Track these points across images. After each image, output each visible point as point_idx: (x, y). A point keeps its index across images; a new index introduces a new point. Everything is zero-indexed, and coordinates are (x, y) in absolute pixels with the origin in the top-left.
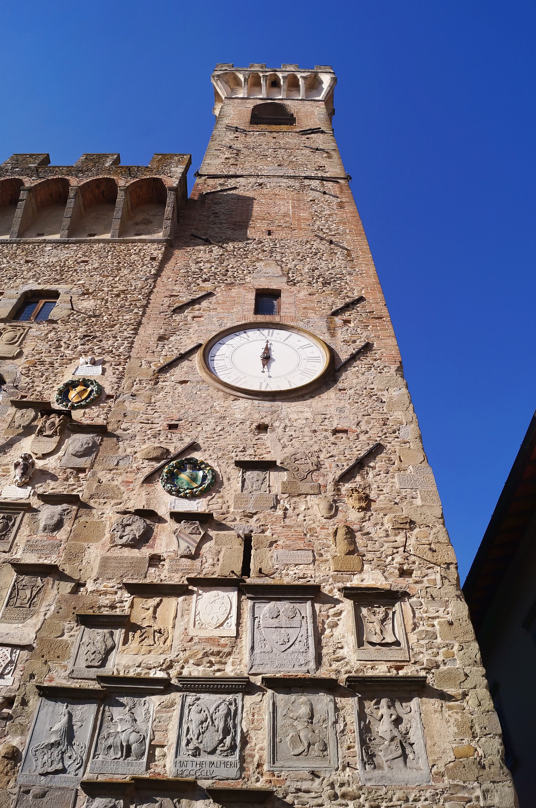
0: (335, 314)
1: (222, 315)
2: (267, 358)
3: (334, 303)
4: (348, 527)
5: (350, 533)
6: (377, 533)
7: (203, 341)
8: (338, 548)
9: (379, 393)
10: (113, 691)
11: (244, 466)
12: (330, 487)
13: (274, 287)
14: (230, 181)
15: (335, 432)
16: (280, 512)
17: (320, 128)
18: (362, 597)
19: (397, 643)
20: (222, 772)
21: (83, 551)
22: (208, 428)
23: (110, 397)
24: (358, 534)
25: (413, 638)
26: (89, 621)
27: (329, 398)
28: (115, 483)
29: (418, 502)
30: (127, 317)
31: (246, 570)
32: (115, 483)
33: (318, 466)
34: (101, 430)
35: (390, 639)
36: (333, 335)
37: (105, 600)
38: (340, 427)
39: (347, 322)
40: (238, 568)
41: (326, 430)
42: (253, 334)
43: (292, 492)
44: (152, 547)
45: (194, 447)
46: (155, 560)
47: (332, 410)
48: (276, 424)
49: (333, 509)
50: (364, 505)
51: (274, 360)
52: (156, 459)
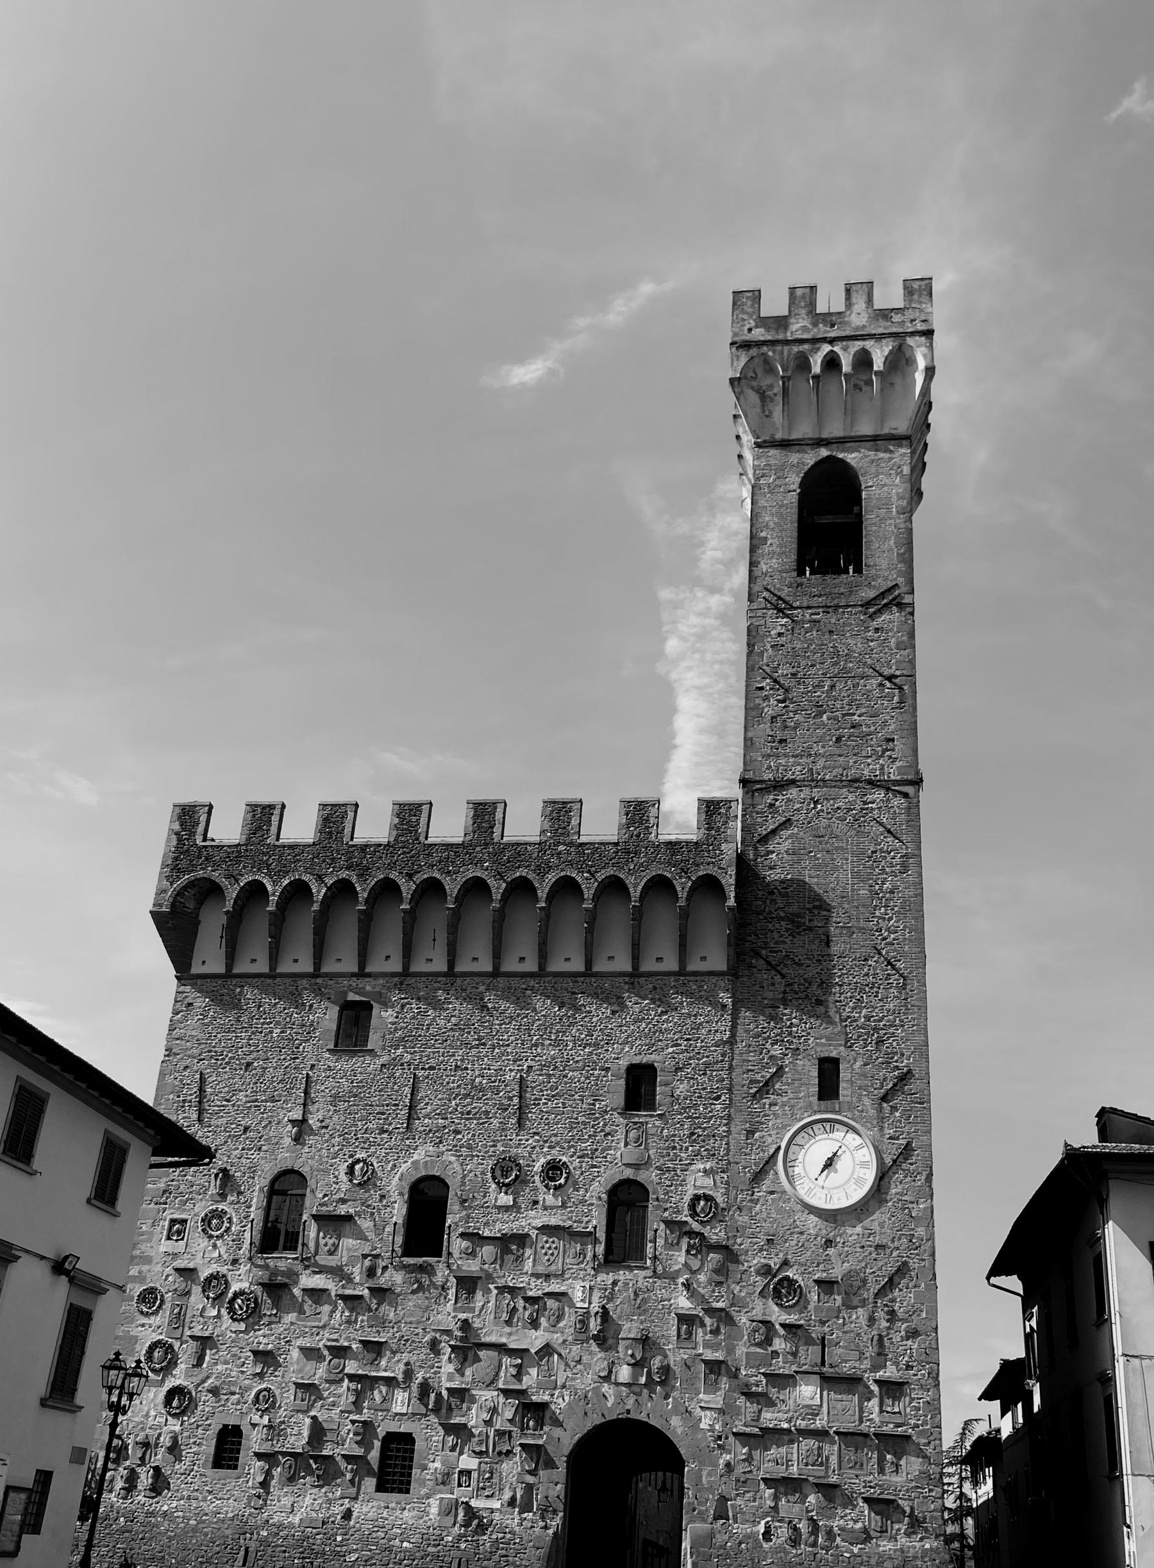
0: (884, 1098)
3: (885, 1080)
4: (880, 1335)
5: (881, 1337)
6: (896, 1338)
8: (870, 1351)
9: (911, 1206)
13: (834, 1054)
15: (878, 1247)
16: (841, 1321)
19: (900, 1413)
21: (734, 1347)
22: (793, 1243)
25: (908, 1410)
29: (924, 1315)
31: (823, 1363)
32: (743, 1294)
33: (864, 1281)
35: (896, 1410)
37: (753, 1380)
39: (894, 1109)
40: (819, 1361)
41: (870, 1246)
45: (785, 1263)
46: (775, 1354)
47: (876, 1227)
49: (872, 1320)
51: (836, 1171)
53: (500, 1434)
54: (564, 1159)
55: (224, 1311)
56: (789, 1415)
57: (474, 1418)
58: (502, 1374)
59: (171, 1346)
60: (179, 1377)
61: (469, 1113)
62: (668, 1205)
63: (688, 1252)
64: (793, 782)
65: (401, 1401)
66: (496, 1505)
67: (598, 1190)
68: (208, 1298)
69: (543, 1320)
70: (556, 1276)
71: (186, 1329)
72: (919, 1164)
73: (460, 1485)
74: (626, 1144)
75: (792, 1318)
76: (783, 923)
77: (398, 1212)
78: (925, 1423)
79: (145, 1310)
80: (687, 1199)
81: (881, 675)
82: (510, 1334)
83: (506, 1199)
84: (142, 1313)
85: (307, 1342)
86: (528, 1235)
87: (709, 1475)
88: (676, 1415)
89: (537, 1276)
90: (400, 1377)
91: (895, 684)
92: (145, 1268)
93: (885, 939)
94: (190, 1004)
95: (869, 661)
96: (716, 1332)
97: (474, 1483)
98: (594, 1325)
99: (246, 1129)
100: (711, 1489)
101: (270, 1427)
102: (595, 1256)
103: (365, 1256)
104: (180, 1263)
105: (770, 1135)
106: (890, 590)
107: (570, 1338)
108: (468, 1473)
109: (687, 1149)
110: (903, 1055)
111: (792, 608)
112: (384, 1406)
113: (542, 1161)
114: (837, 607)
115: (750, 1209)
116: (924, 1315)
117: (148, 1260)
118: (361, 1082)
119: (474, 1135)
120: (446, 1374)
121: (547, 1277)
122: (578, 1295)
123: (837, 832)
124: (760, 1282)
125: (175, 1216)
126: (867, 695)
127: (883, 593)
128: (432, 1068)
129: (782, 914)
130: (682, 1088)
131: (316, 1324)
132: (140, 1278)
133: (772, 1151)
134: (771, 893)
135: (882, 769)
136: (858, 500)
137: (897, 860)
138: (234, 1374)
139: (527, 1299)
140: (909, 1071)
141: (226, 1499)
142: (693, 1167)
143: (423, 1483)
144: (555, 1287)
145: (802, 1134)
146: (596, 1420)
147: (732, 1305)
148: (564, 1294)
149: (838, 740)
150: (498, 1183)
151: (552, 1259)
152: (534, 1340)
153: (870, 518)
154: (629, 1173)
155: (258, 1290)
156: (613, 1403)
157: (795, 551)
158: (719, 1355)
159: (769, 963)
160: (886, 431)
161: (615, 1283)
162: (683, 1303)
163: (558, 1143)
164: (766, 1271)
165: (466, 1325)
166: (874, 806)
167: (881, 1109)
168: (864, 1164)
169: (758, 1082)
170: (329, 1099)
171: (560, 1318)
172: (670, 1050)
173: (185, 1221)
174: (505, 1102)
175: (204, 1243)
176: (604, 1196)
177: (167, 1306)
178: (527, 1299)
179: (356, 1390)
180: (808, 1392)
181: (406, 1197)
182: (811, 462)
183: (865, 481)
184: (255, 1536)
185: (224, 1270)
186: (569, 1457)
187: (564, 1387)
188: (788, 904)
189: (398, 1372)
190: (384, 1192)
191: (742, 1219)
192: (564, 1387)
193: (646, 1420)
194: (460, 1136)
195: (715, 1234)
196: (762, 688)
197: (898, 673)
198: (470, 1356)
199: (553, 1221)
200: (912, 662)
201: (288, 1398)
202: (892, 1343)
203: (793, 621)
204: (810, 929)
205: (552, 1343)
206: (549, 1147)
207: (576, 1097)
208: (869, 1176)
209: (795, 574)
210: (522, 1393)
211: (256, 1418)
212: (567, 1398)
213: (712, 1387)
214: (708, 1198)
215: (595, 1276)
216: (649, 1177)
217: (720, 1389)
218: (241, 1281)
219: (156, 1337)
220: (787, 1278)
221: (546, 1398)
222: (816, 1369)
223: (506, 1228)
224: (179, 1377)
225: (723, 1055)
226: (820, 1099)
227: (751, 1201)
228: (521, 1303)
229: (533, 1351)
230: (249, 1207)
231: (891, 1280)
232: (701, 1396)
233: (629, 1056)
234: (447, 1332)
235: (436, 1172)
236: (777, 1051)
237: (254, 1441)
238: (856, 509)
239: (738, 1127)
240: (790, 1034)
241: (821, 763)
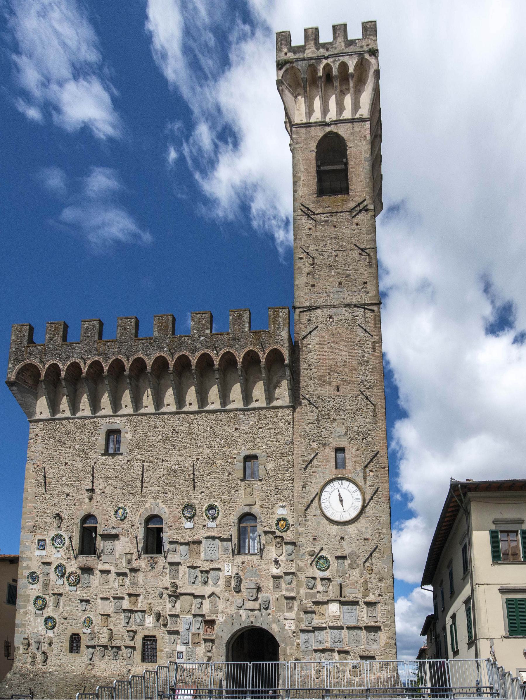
0: (366, 467)
1: (323, 470)
2: (341, 501)
7: (318, 491)
10: (315, 629)
11: (338, 558)
12: (362, 565)
13: (342, 445)
14: (314, 314)
15: (365, 539)
17: (365, 200)
18: (369, 604)
20: (339, 646)
23: (292, 525)
24: (369, 583)
26: (306, 612)
27: (362, 520)
28: (302, 565)
30: (288, 475)
31: (341, 596)
34: (294, 544)
36: (365, 483)
37: (308, 605)
38: (366, 537)
41: (361, 539)
42: (336, 484)
43: (351, 567)
44: (316, 589)
45: (322, 549)
47: (363, 529)
48: (346, 537)
50: (370, 572)
52: (312, 555)
53: (194, 634)
54: (216, 504)
55: (66, 582)
56: (326, 621)
57: (182, 627)
58: (193, 607)
59: (44, 598)
60: (49, 612)
61: (170, 483)
62: (266, 524)
63: (276, 545)
64: (319, 307)
65: (149, 621)
66: (195, 666)
67: (234, 518)
68: (58, 576)
69: (210, 581)
71: (50, 590)
72: (383, 497)
73: (178, 658)
74: (245, 495)
75: (326, 574)
76: (316, 380)
77: (141, 533)
78: (387, 620)
79: (32, 582)
80: (275, 521)
81: (359, 248)
82: (196, 589)
83: (190, 525)
84: (30, 583)
85: (105, 595)
87: (290, 649)
88: (274, 623)
90: (147, 610)
91: (366, 253)
92: (29, 563)
93: (365, 386)
94: (37, 435)
95: (354, 241)
96: (290, 583)
97: (184, 657)
98: (233, 584)
99: (68, 495)
100: (291, 656)
101: (91, 633)
103: (126, 554)
104: (45, 560)
105: (313, 488)
106: (362, 203)
107: (224, 590)
108: (182, 652)
109: (274, 496)
110: (375, 444)
111: (314, 214)
112: (141, 624)
113: (206, 505)
114: (337, 212)
115: (305, 524)
116: (386, 570)
117: (30, 559)
118: (118, 469)
119: (173, 494)
120: (167, 607)
123: (341, 332)
124: (310, 559)
125: (40, 538)
126: (353, 259)
127: (359, 205)
128: (151, 462)
129: (316, 376)
130: (271, 466)
131: (108, 587)
132: (28, 568)
133: (314, 495)
134: (310, 365)
135: (361, 298)
136: (345, 156)
137: (370, 345)
138: (73, 611)
139: (202, 572)
140: (378, 453)
141: (77, 664)
142: (277, 505)
143: (161, 658)
144: (216, 565)
145: (329, 486)
146: (237, 627)
147: (299, 570)
149: (340, 284)
150: (185, 517)
152: (207, 590)
153: (351, 164)
154: (247, 510)
155: (79, 571)
156: (245, 619)
157: (315, 183)
158: (292, 594)
159: (309, 401)
160: (357, 116)
161: (243, 563)
162: (275, 571)
163: (213, 496)
164: (312, 554)
166: (358, 318)
167: (365, 472)
168: (357, 500)
169: (306, 461)
170: (104, 479)
172: (264, 447)
173: (44, 540)
174: (187, 477)
175: (54, 550)
176: (236, 521)
177: (41, 580)
178: (202, 572)
179: (128, 617)
180: (334, 608)
181: (143, 525)
182: (321, 135)
183: (349, 144)
184: (89, 682)
185: (64, 563)
186: (226, 644)
187: (222, 612)
188: (319, 370)
189: (146, 608)
190: (133, 523)
191: (301, 529)
192: (222, 612)
193: (260, 626)
194: (167, 495)
195: (288, 536)
196: (301, 258)
197: (368, 247)
199: (213, 534)
200: (375, 240)
201: (97, 620)
202: (372, 585)
203: (315, 221)
204: (329, 383)
205: (215, 592)
206: (209, 498)
207: (220, 473)
208: (359, 505)
209: (316, 196)
210: (203, 616)
211: (85, 631)
212: (224, 618)
213: (290, 609)
214: (284, 520)
216: (256, 510)
217: (294, 610)
218: (72, 567)
219: (37, 594)
220: (322, 557)
221: (213, 617)
222: (337, 599)
224: (49, 612)
225: (289, 448)
226: (336, 468)
227: (305, 520)
228: (199, 574)
229: (206, 596)
230: (72, 532)
231: (371, 555)
232: (285, 614)
233: (245, 451)
234: (167, 589)
235: (156, 513)
236: (314, 445)
237: (85, 641)
238: (344, 160)
239: (298, 485)
240: (321, 436)
241: (332, 296)
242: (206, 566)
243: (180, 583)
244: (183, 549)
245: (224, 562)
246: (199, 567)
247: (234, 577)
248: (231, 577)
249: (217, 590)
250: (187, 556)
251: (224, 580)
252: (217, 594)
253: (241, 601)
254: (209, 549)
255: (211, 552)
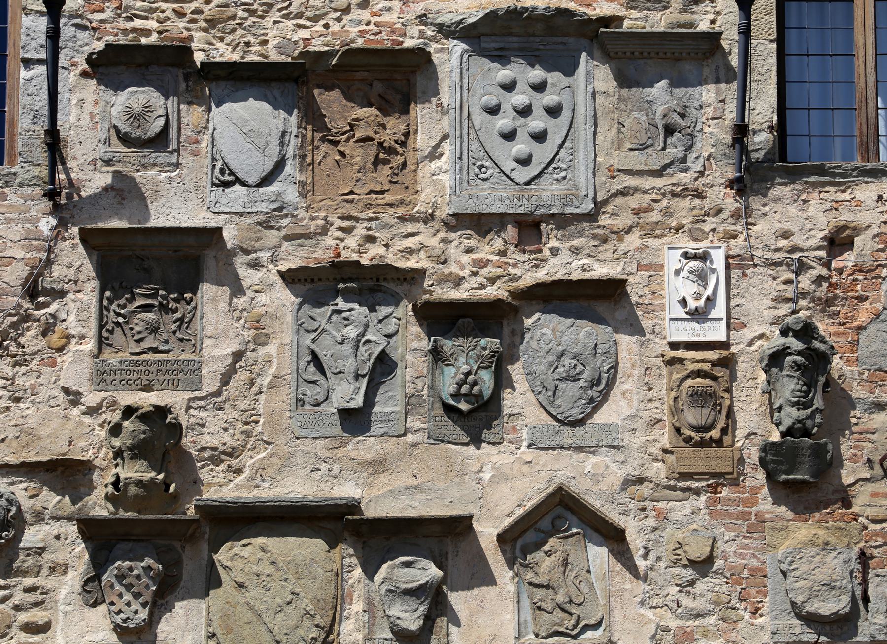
69: (520, 400)
70: (563, 221)
82: (377, 466)
86: (420, 59)
89: (480, 224)
98: (756, 416)
102: (741, 130)
107: (658, 471)
121: (529, 228)
122: (672, 289)
144: (563, 260)
148: (613, 289)
151: (542, 153)
165: (158, 438)
171: (601, 388)
198: (190, 569)
215: (744, 215)
223: (318, 39)
228: (412, 343)
229: (487, 532)
242: (473, 272)
243: (207, 430)
244: (246, 127)
245: (651, 231)
246: (418, 275)
247: (775, 359)
248: (728, 363)
249: (595, 477)
250: (286, 189)
251: (661, 386)
252: (595, 502)
253: (836, 565)
254: (504, 122)
255: (520, 147)
